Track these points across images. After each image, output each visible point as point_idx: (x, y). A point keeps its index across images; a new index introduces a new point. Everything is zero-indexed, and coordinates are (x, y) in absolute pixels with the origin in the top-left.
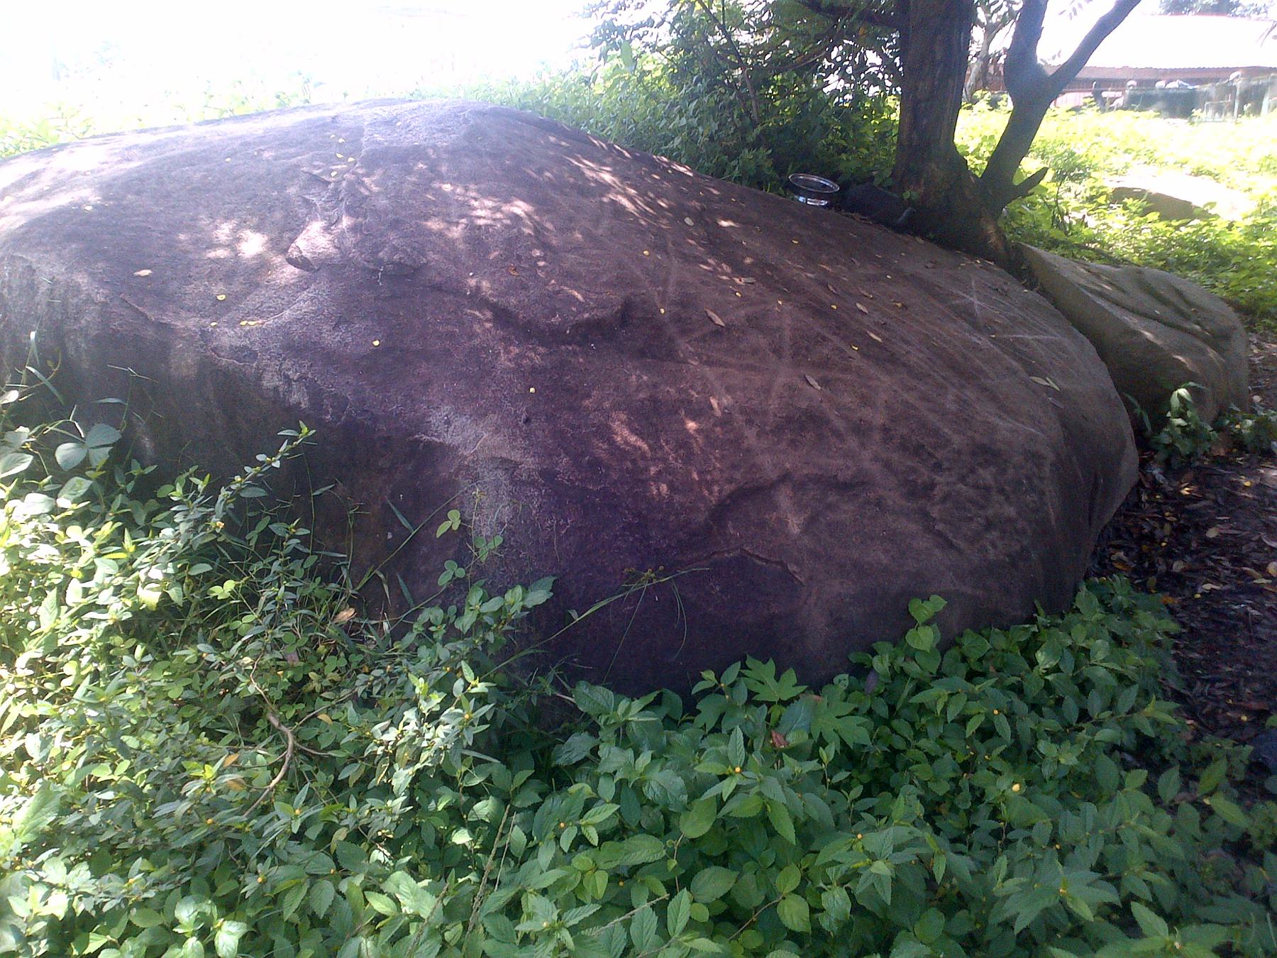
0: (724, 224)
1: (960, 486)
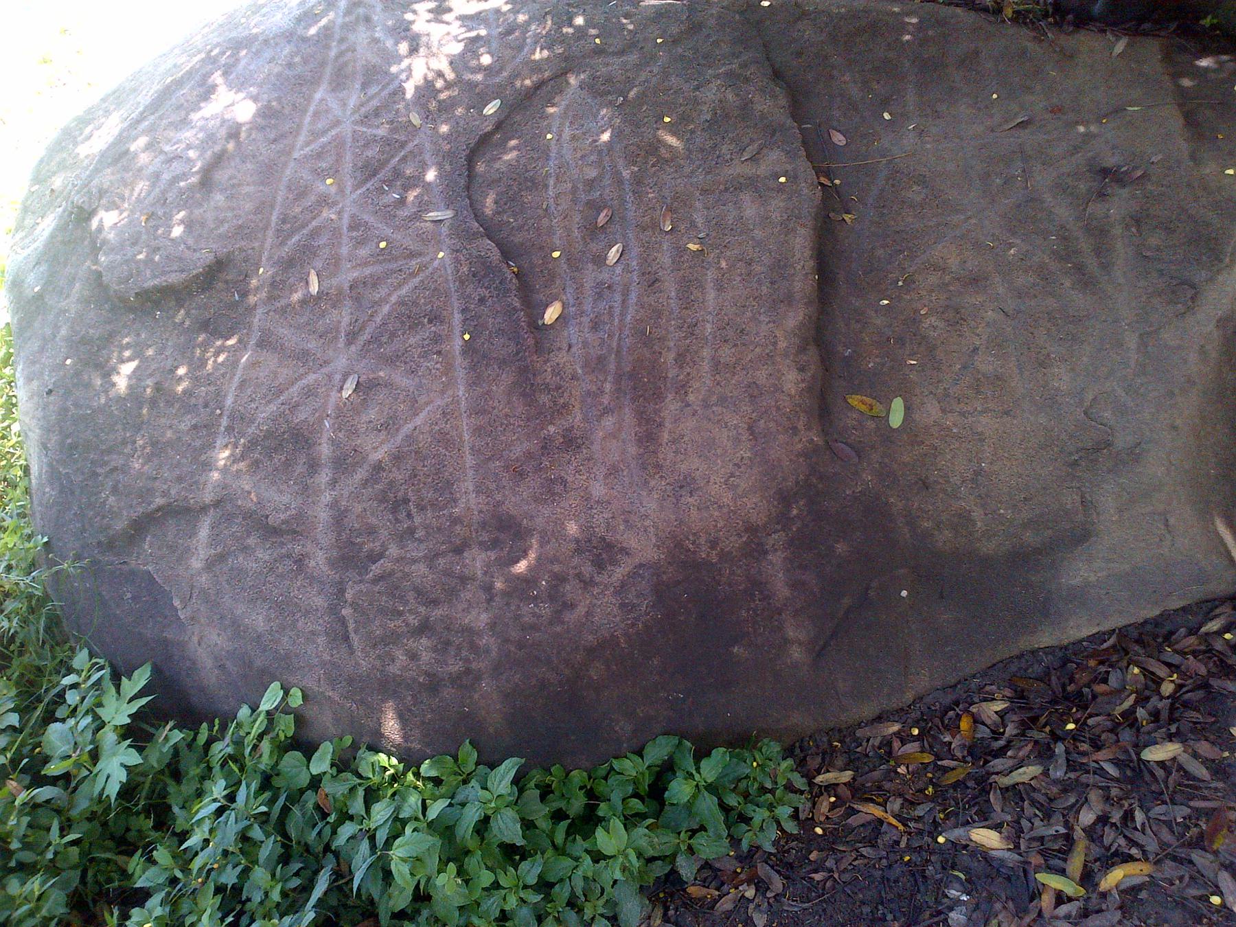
1: (422, 568)
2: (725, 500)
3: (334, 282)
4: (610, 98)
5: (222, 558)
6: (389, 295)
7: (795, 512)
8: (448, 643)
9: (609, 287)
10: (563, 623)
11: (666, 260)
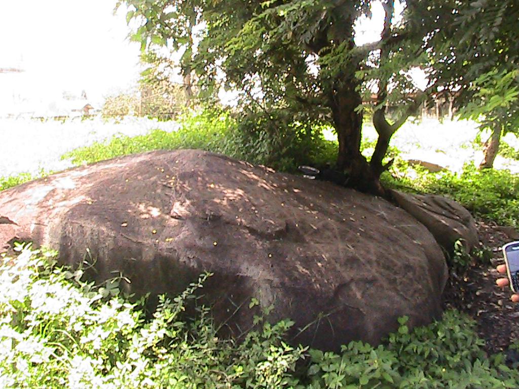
0: (296, 191)
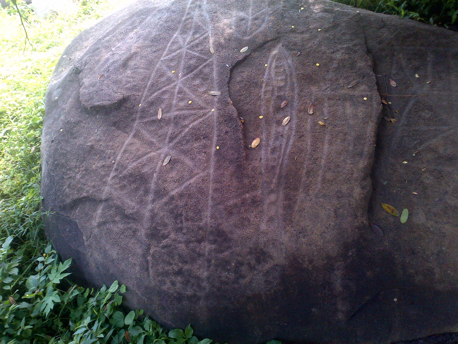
2: (319, 243)
3: (168, 115)
4: (294, 52)
5: (104, 223)
6: (189, 124)
7: (350, 254)
8: (188, 282)
9: (281, 135)
10: (238, 283)
11: (308, 127)
